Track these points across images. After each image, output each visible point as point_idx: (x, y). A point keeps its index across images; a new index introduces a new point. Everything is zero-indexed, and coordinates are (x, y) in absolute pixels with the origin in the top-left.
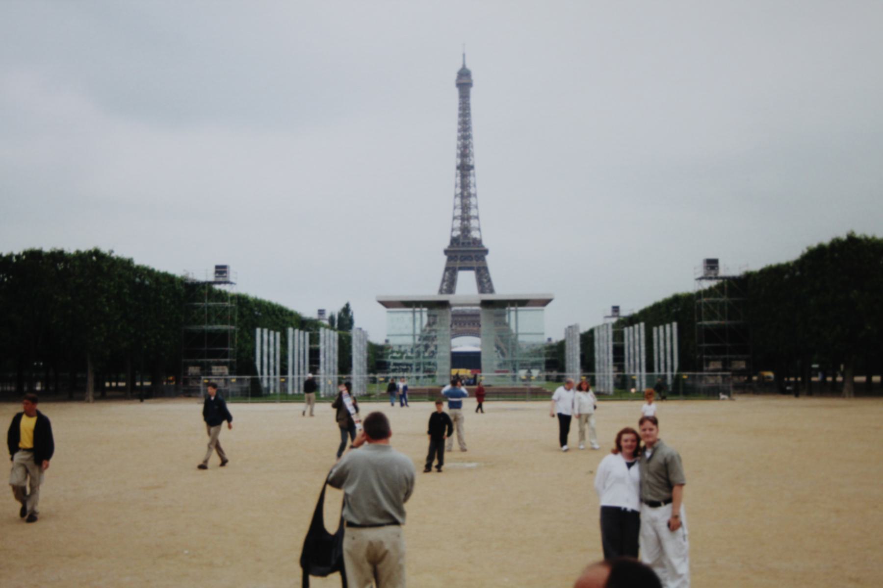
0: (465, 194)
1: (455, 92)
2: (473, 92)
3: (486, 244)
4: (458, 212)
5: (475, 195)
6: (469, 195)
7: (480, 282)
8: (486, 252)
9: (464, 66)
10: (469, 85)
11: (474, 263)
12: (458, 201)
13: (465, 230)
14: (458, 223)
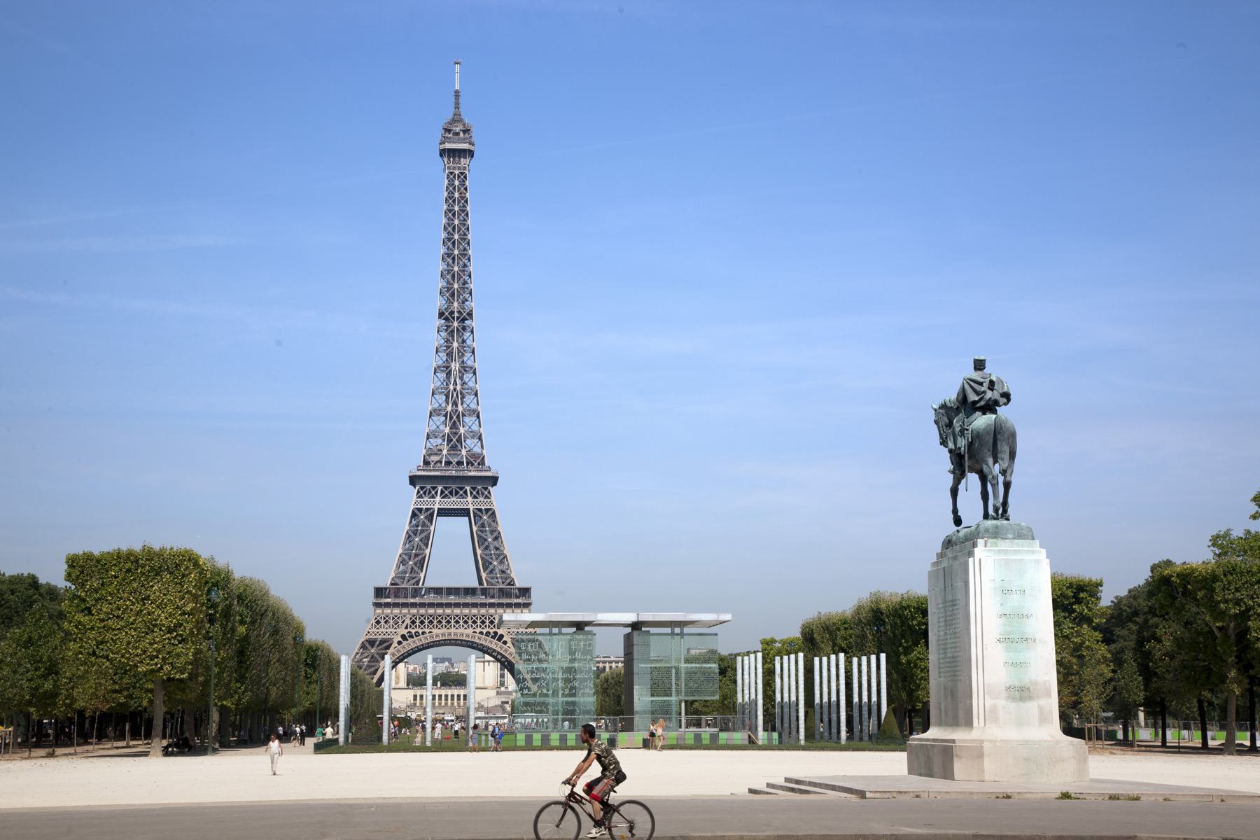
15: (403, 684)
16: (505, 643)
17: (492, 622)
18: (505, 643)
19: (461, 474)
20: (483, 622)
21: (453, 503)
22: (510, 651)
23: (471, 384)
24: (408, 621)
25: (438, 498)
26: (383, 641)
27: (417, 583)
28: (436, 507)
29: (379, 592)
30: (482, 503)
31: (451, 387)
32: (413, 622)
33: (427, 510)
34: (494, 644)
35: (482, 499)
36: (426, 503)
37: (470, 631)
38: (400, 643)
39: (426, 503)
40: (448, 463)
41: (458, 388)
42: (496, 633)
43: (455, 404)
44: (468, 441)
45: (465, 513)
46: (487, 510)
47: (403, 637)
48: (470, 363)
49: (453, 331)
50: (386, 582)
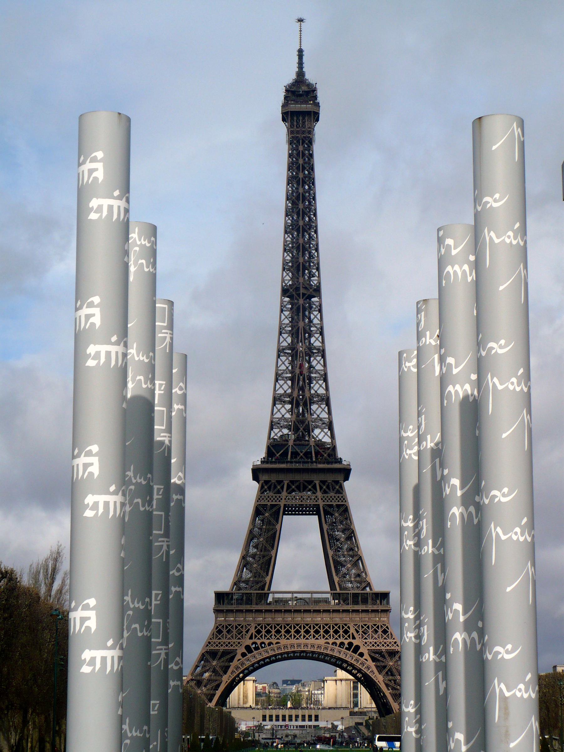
0: (301, 347)
1: (281, 131)
2: (321, 131)
3: (344, 453)
4: (285, 387)
5: (322, 353)
6: (310, 352)
7: (328, 540)
8: (346, 473)
9: (301, 73)
10: (316, 116)
11: (320, 498)
12: (285, 363)
13: (302, 426)
14: (284, 411)
15: (251, 702)
16: (361, 655)
17: (346, 632)
18: (361, 655)
19: (309, 466)
20: (336, 632)
21: (296, 498)
22: (370, 667)
23: (319, 367)
24: (253, 631)
25: (284, 494)
26: (225, 653)
27: (263, 588)
28: (282, 504)
29: (220, 597)
30: (332, 499)
31: (297, 371)
32: (259, 632)
33: (273, 506)
34: (349, 657)
35: (332, 494)
36: (271, 498)
37: (322, 641)
38: (244, 655)
39: (271, 498)
40: (295, 454)
41: (305, 372)
42: (350, 644)
43: (302, 389)
44: (317, 431)
45: (314, 510)
46: (338, 506)
47: (248, 648)
48: (317, 344)
49: (298, 309)
50: (226, 586)
